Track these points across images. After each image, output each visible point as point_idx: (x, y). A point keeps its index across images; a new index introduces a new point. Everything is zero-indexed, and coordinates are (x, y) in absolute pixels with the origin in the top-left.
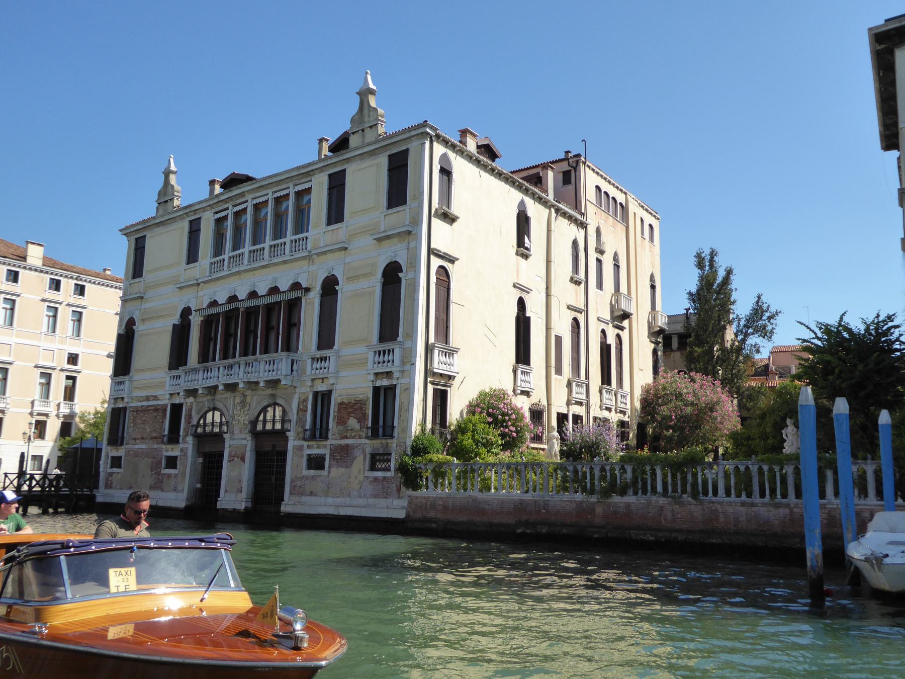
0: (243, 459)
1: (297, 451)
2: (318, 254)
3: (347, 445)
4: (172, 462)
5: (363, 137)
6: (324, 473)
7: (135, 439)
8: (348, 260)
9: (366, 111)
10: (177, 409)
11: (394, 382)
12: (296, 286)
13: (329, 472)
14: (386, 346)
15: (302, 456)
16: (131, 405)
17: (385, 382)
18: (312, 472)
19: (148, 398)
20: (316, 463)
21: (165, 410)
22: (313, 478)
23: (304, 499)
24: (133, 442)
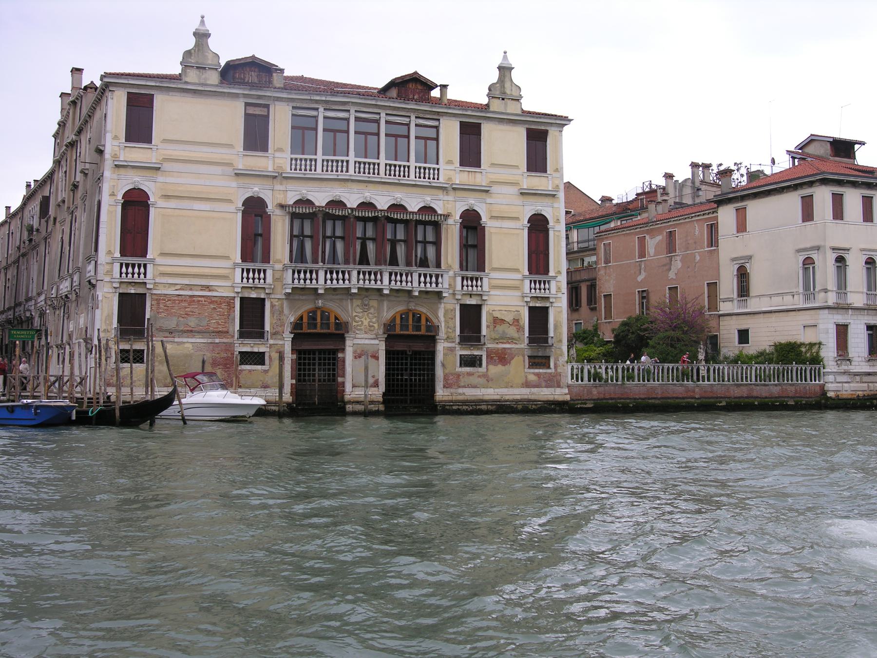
1: (447, 351)
2: (454, 189)
4: (258, 358)
5: (506, 104)
8: (489, 201)
9: (507, 85)
12: (427, 209)
16: (155, 292)
18: (468, 369)
19: (190, 287)
20: (471, 362)
21: (231, 307)
23: (460, 390)
24: (167, 334)
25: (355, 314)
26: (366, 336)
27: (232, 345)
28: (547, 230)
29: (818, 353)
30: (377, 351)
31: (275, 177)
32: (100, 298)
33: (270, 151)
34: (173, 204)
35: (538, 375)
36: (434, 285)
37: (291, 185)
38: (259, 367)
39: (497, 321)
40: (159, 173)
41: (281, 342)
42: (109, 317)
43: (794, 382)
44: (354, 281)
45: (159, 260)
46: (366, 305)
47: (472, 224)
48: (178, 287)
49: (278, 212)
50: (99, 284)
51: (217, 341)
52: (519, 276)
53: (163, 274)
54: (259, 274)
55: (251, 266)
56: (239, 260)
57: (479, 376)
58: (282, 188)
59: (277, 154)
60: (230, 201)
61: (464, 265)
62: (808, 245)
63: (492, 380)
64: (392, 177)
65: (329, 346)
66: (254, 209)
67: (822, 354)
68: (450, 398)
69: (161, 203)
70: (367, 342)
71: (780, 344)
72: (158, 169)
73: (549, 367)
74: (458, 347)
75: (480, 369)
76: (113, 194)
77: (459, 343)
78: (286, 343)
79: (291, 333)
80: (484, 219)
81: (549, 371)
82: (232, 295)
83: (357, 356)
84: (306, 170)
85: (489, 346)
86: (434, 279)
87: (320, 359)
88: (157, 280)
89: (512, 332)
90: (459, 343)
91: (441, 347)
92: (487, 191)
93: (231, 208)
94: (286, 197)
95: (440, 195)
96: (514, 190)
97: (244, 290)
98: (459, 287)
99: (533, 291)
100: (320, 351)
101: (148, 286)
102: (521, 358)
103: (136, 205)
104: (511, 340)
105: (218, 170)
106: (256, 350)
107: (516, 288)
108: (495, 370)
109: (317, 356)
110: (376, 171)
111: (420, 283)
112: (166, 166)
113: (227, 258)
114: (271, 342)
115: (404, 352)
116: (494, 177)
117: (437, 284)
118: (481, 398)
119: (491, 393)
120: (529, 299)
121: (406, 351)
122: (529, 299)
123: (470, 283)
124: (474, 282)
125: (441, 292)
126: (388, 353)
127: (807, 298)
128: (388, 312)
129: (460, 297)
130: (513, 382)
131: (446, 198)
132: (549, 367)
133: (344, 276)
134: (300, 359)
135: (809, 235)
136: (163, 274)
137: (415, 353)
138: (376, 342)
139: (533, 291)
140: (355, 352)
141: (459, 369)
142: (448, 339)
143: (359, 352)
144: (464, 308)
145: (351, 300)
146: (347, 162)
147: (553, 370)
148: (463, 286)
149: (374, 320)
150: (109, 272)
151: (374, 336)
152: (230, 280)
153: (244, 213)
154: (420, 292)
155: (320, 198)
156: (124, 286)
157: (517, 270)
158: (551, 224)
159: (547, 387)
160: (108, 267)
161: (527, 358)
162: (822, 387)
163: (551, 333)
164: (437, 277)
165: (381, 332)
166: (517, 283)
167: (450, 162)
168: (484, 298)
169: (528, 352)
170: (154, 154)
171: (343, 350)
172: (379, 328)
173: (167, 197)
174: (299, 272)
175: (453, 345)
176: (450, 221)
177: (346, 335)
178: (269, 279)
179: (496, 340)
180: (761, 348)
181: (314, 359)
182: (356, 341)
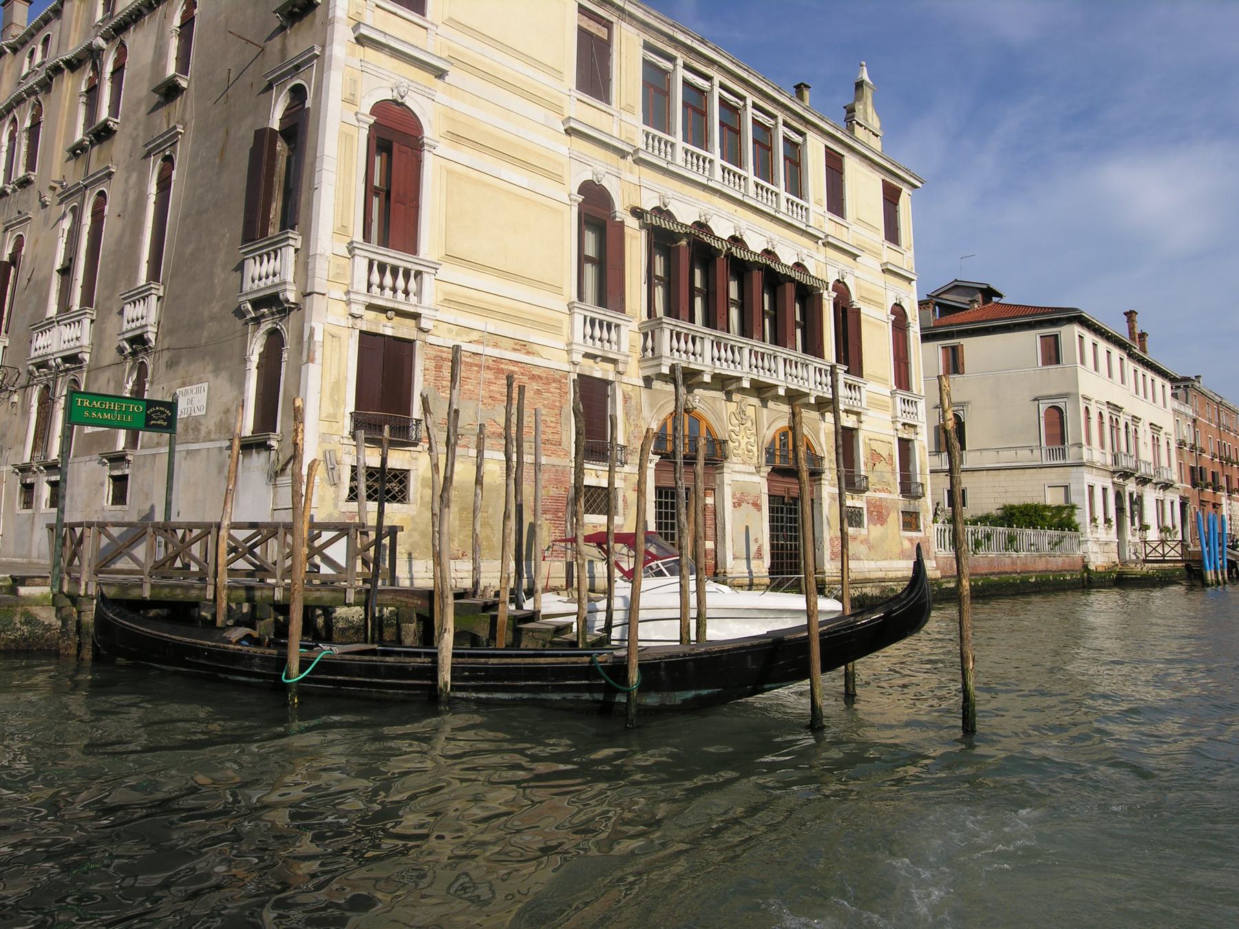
0: (757, 506)
6: (863, 531)
19: (495, 339)
29: (1070, 516)
30: (759, 497)
32: (318, 337)
34: (465, 155)
37: (648, 176)
42: (337, 386)
43: (1034, 552)
48: (475, 336)
62: (1054, 393)
67: (1077, 519)
69: (444, 148)
70: (747, 478)
71: (1012, 507)
76: (350, 101)
83: (737, 505)
103: (395, 141)
112: (454, 75)
126: (772, 498)
127: (1051, 453)
135: (1052, 380)
138: (756, 479)
158: (910, 320)
162: (1083, 558)
167: (818, 203)
180: (986, 512)
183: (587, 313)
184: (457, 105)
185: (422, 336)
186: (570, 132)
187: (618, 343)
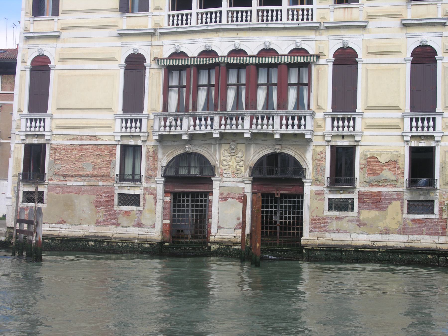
1: (315, 195)
2: (327, 28)
3: (380, 192)
7: (65, 176)
10: (131, 152)
11: (433, 144)
12: (298, 51)
13: (359, 214)
14: (426, 115)
15: (324, 200)
16: (53, 142)
17: (422, 144)
18: (337, 213)
22: (337, 218)
23: (328, 235)
24: (62, 178)
25: (223, 158)
26: (232, 179)
27: (111, 189)
28: (435, 62)
31: (152, 34)
32: (12, 148)
33: (150, 11)
34: (69, 65)
35: (419, 221)
36: (296, 127)
38: (134, 208)
39: (372, 161)
40: (61, 40)
41: (153, 185)
44: (217, 127)
45: (56, 115)
46: (233, 149)
47: (346, 60)
49: (154, 66)
50: (12, 136)
51: (101, 184)
52: (399, 114)
53: (59, 127)
54: (136, 123)
55: (419, 115)
56: (408, 110)
57: (349, 221)
58: (160, 43)
59: (156, 13)
60: (113, 59)
61: (337, 105)
63: (365, 225)
64: (295, 21)
65: (201, 189)
66: (135, 64)
68: (316, 242)
69: (59, 66)
72: (58, 37)
73: (433, 213)
74: (326, 191)
75: (350, 214)
76: (23, 62)
77: (328, 187)
78: (158, 186)
79: (162, 177)
80: (361, 55)
81: (431, 217)
82: (114, 143)
83: (223, 199)
84: (177, 24)
85: (362, 189)
86: (296, 121)
87: (193, 201)
88: (55, 132)
89: (387, 174)
90: (328, 187)
91: (308, 190)
92: (365, 27)
93: (115, 65)
94: (162, 51)
95: (312, 35)
96: (396, 22)
97: (123, 139)
98: (328, 127)
99: (414, 129)
100: (193, 194)
101: (47, 137)
102: (399, 203)
104: (392, 183)
105: (105, 32)
106: (132, 192)
107: (396, 127)
108: (368, 215)
109: (190, 198)
110: (249, 18)
111: (281, 125)
112: (64, 34)
113: (110, 110)
114: (145, 185)
115: (272, 195)
116: (372, 11)
117: (299, 126)
118: (349, 243)
119: (360, 238)
120: (408, 139)
121: (274, 194)
122: (408, 139)
123: (341, 123)
124: (346, 123)
125: (304, 135)
128: (255, 154)
129: (329, 139)
130: (389, 227)
131: (318, 37)
132: (433, 213)
133: (257, 122)
134: (175, 201)
136: (59, 127)
137: (282, 195)
138: (242, 185)
139: (414, 129)
140: (221, 194)
141: (327, 213)
142: (316, 181)
143: (225, 194)
144: (335, 150)
145: (220, 144)
146: (221, 12)
147: (438, 217)
148: (333, 127)
149: (241, 163)
150: (18, 127)
151: (240, 179)
152: (112, 131)
153: (126, 69)
154: (282, 135)
155: (193, 47)
156: (30, 138)
157: (396, 108)
159: (427, 234)
160: (18, 122)
161: (406, 203)
163: (437, 175)
164: (300, 119)
165: (247, 174)
166: (397, 122)
168: (357, 138)
169: (407, 197)
170: (56, 24)
171: (211, 192)
172: (245, 170)
173: (63, 60)
174: (417, 120)
175: (321, 188)
176: (322, 61)
177: (213, 178)
178: (144, 128)
179: (371, 184)
181: (188, 201)
182: (222, 184)
183: (122, 118)
184: (67, 45)
185: (48, 142)
186: (121, 35)
187: (140, 128)
